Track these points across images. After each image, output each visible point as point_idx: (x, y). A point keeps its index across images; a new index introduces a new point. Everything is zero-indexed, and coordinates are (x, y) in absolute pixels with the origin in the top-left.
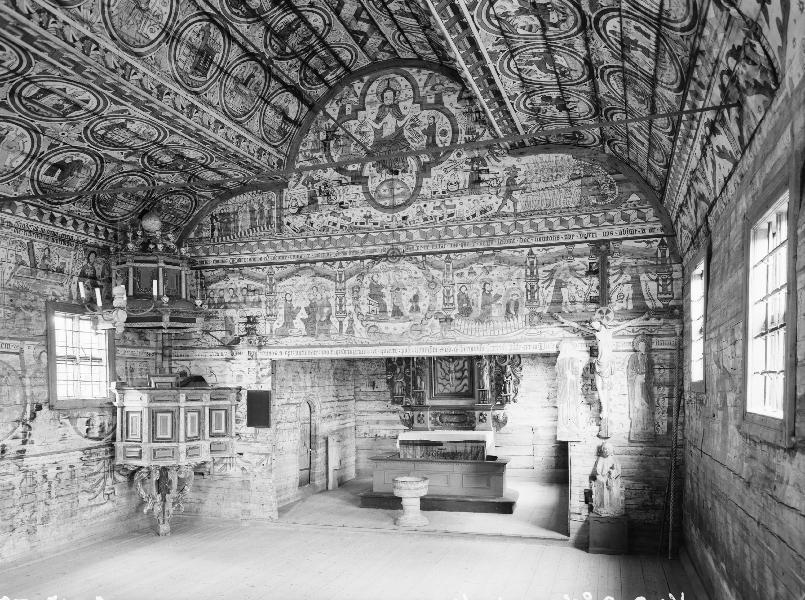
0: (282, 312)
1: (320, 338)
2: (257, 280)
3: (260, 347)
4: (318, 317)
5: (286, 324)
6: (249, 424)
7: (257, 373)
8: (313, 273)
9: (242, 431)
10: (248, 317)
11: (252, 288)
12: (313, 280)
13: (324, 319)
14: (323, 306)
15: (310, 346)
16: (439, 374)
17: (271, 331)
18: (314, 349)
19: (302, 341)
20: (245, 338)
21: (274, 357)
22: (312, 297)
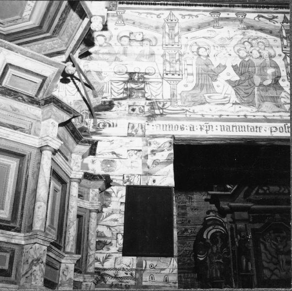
0: (193, 69)
1: (263, 108)
2: (148, 27)
3: (151, 117)
4: (257, 80)
5: (199, 86)
6: (127, 251)
7: (146, 157)
8: (242, 26)
9: (107, 265)
10: (131, 74)
11: (139, 38)
12: (244, 34)
13: (269, 82)
14: (263, 67)
15: (246, 119)
16: (264, 257)
17: (173, 95)
18: (255, 124)
19: (231, 111)
20: (123, 102)
21: (179, 133)
22: (243, 53)
